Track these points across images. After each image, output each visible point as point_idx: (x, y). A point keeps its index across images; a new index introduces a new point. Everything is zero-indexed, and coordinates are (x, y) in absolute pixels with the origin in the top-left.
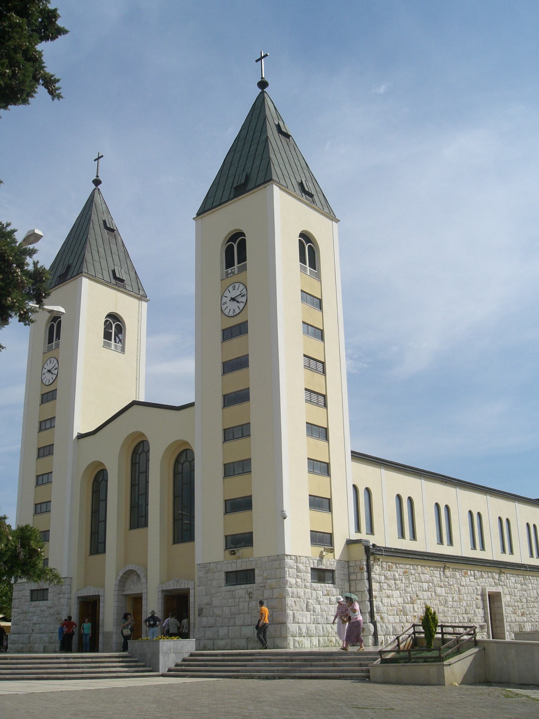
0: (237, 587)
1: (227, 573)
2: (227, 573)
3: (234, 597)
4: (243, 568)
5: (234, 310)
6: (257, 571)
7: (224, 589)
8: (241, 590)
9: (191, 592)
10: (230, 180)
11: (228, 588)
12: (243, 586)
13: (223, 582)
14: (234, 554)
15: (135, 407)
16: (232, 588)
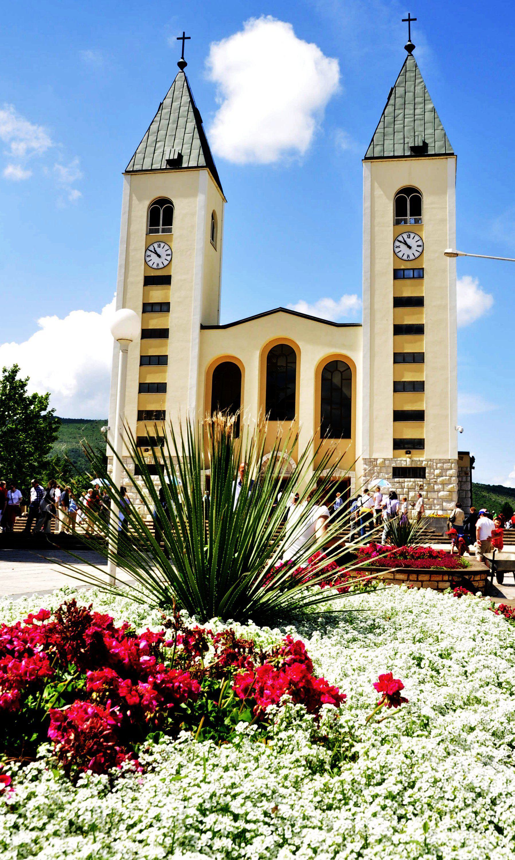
0: (406, 480)
1: (394, 468)
2: (394, 469)
3: (403, 488)
4: (413, 466)
5: (408, 256)
6: (427, 471)
7: (392, 480)
8: (409, 482)
9: (353, 481)
10: (399, 136)
11: (397, 479)
12: (412, 480)
13: (391, 474)
14: (410, 453)
15: (281, 313)
16: (401, 480)
